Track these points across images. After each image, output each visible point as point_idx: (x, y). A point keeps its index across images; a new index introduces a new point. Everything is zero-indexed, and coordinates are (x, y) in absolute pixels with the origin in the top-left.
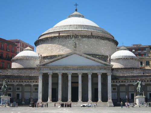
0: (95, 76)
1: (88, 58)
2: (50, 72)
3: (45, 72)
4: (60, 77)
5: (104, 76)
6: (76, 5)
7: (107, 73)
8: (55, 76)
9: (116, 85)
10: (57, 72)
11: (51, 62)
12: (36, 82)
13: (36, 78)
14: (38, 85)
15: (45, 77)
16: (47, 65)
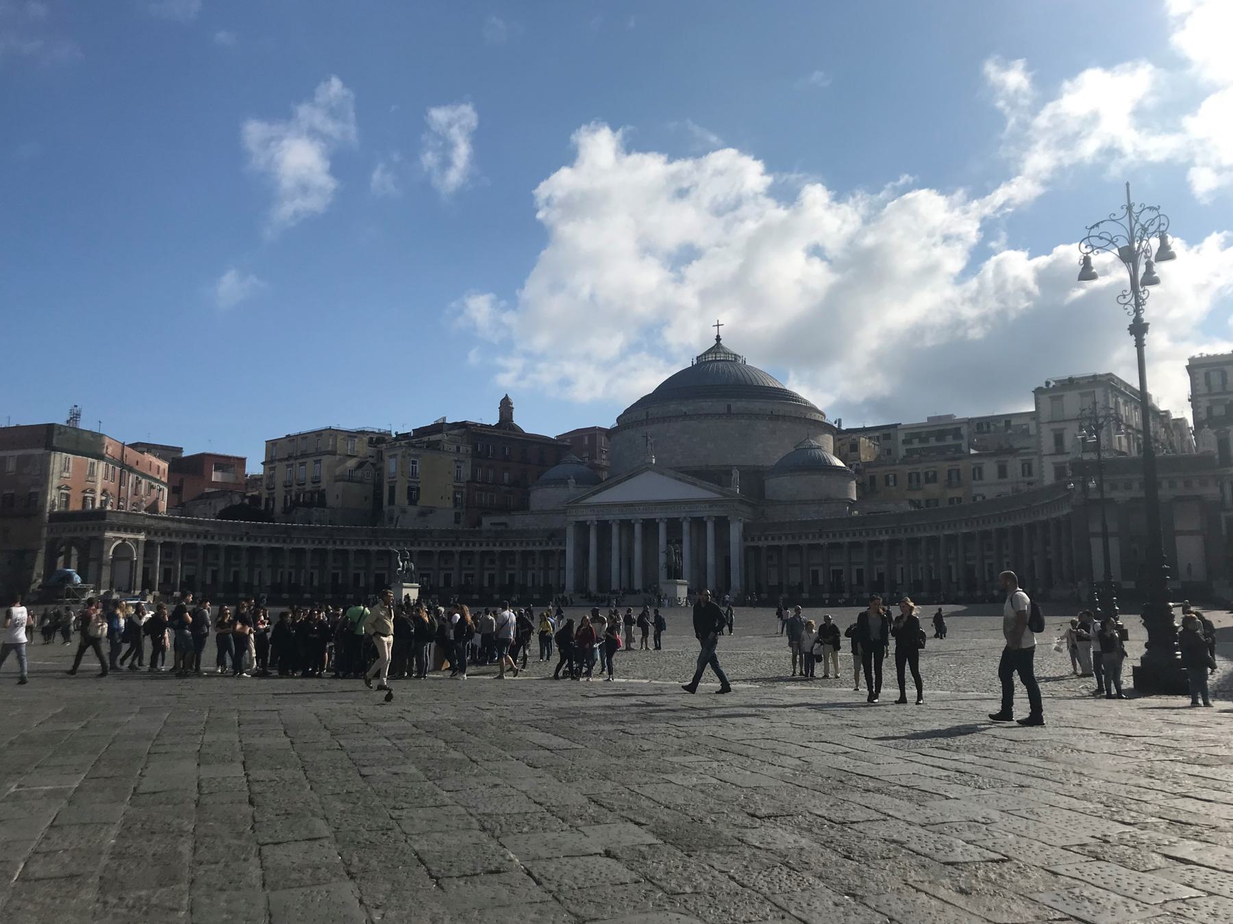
0: (699, 523)
1: (680, 479)
2: (591, 517)
3: (581, 519)
4: (615, 529)
5: (722, 524)
6: (718, 325)
7: (727, 517)
8: (604, 527)
9: (757, 549)
10: (607, 517)
11: (594, 494)
12: (560, 544)
13: (556, 535)
14: (563, 553)
15: (582, 527)
16: (586, 501)
